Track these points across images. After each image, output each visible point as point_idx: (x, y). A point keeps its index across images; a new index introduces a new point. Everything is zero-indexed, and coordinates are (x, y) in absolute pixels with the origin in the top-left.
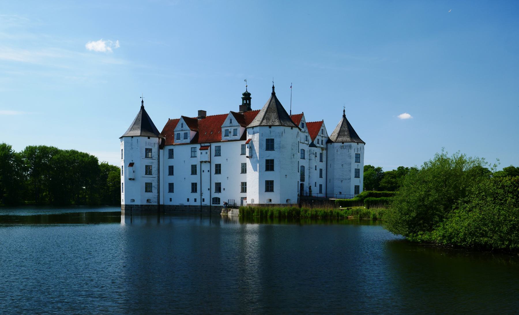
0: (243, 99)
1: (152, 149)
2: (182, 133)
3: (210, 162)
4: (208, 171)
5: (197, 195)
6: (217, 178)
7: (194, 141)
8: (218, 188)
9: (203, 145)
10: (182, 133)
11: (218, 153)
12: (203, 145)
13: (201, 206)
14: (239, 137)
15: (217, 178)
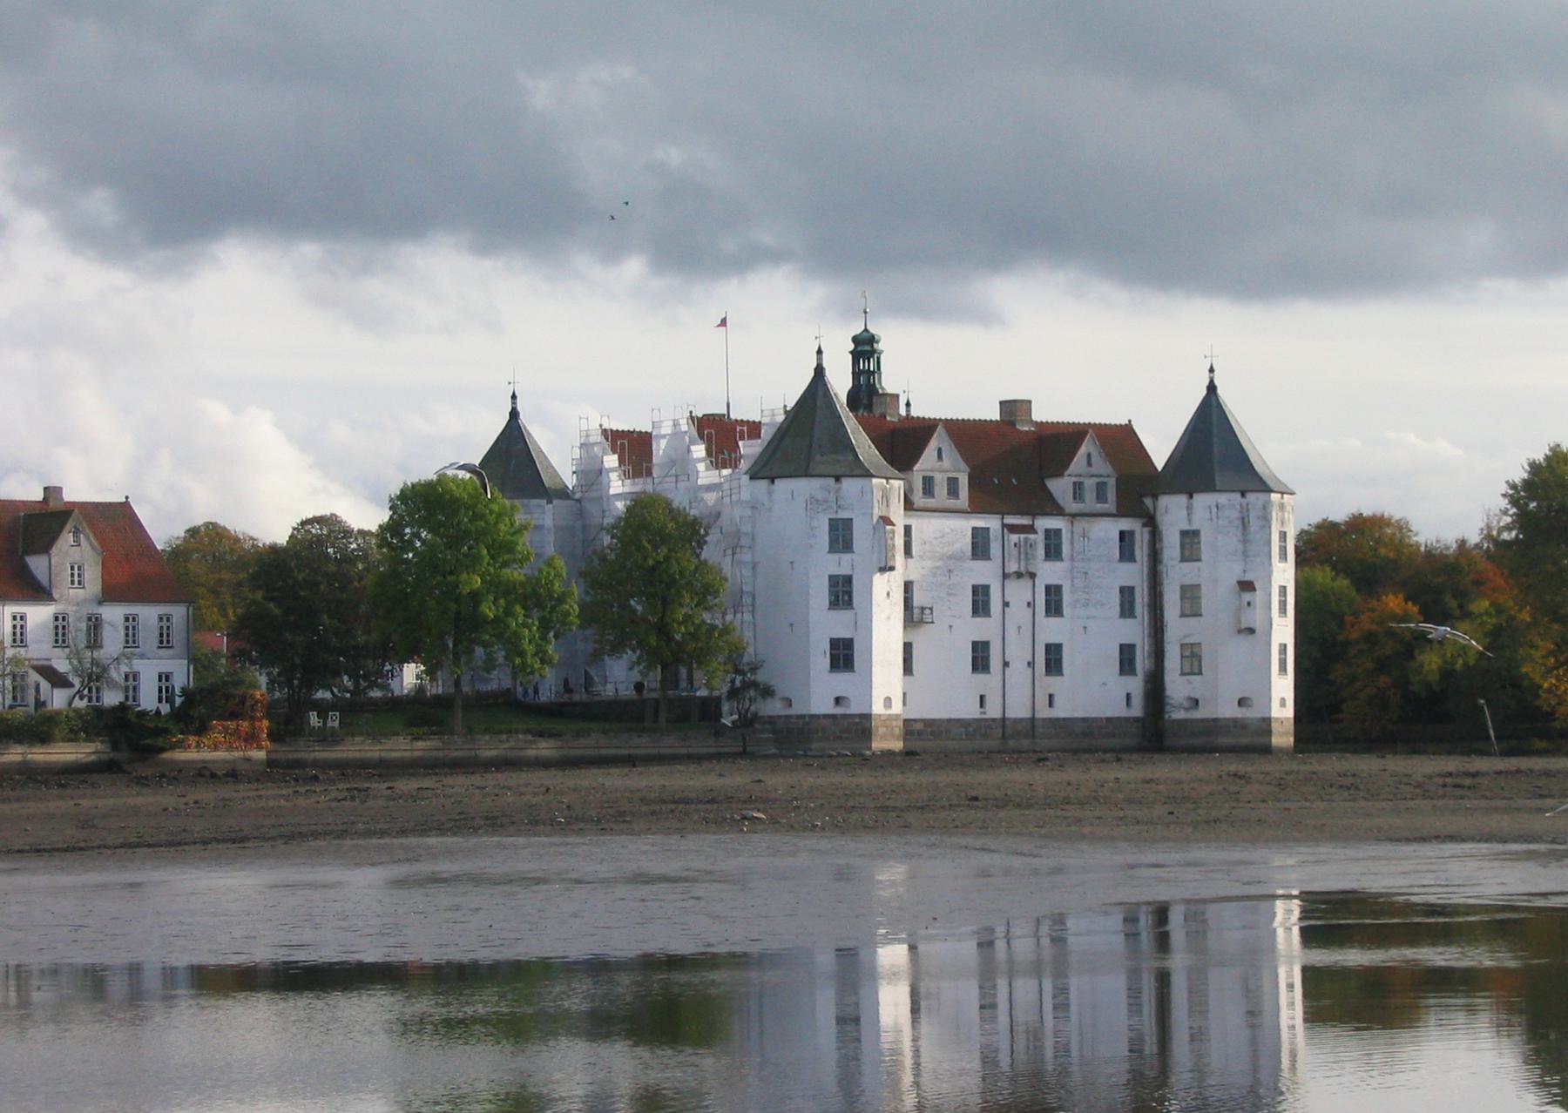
0: (856, 355)
1: (851, 520)
2: (940, 480)
3: (1033, 576)
4: (1029, 604)
5: (989, 683)
6: (1052, 629)
7: (976, 507)
8: (1054, 659)
9: (1010, 520)
10: (940, 480)
11: (1053, 550)
12: (1010, 520)
13: (1004, 719)
14: (1110, 506)
15: (1052, 629)
